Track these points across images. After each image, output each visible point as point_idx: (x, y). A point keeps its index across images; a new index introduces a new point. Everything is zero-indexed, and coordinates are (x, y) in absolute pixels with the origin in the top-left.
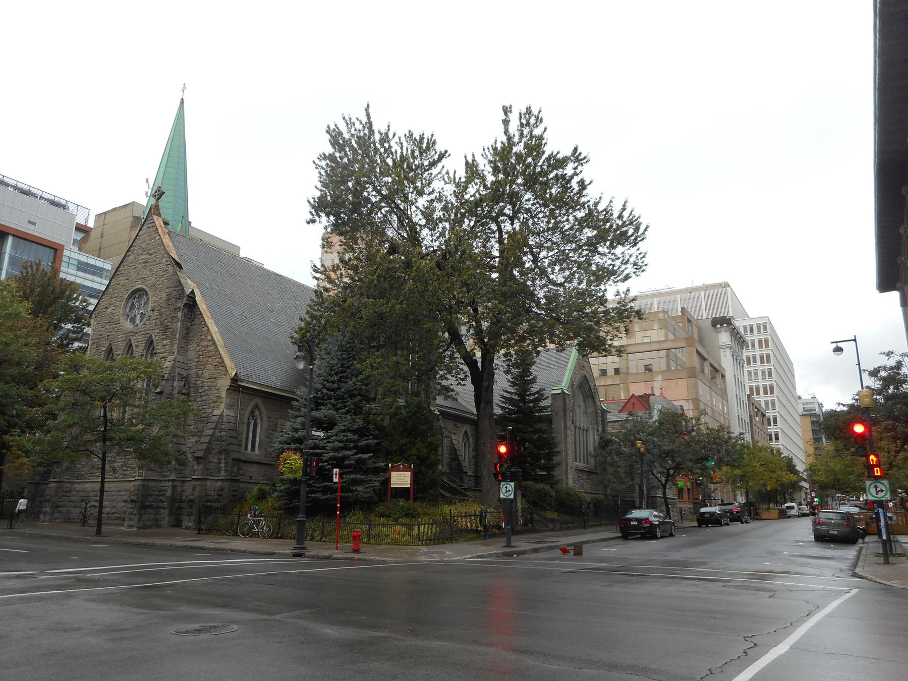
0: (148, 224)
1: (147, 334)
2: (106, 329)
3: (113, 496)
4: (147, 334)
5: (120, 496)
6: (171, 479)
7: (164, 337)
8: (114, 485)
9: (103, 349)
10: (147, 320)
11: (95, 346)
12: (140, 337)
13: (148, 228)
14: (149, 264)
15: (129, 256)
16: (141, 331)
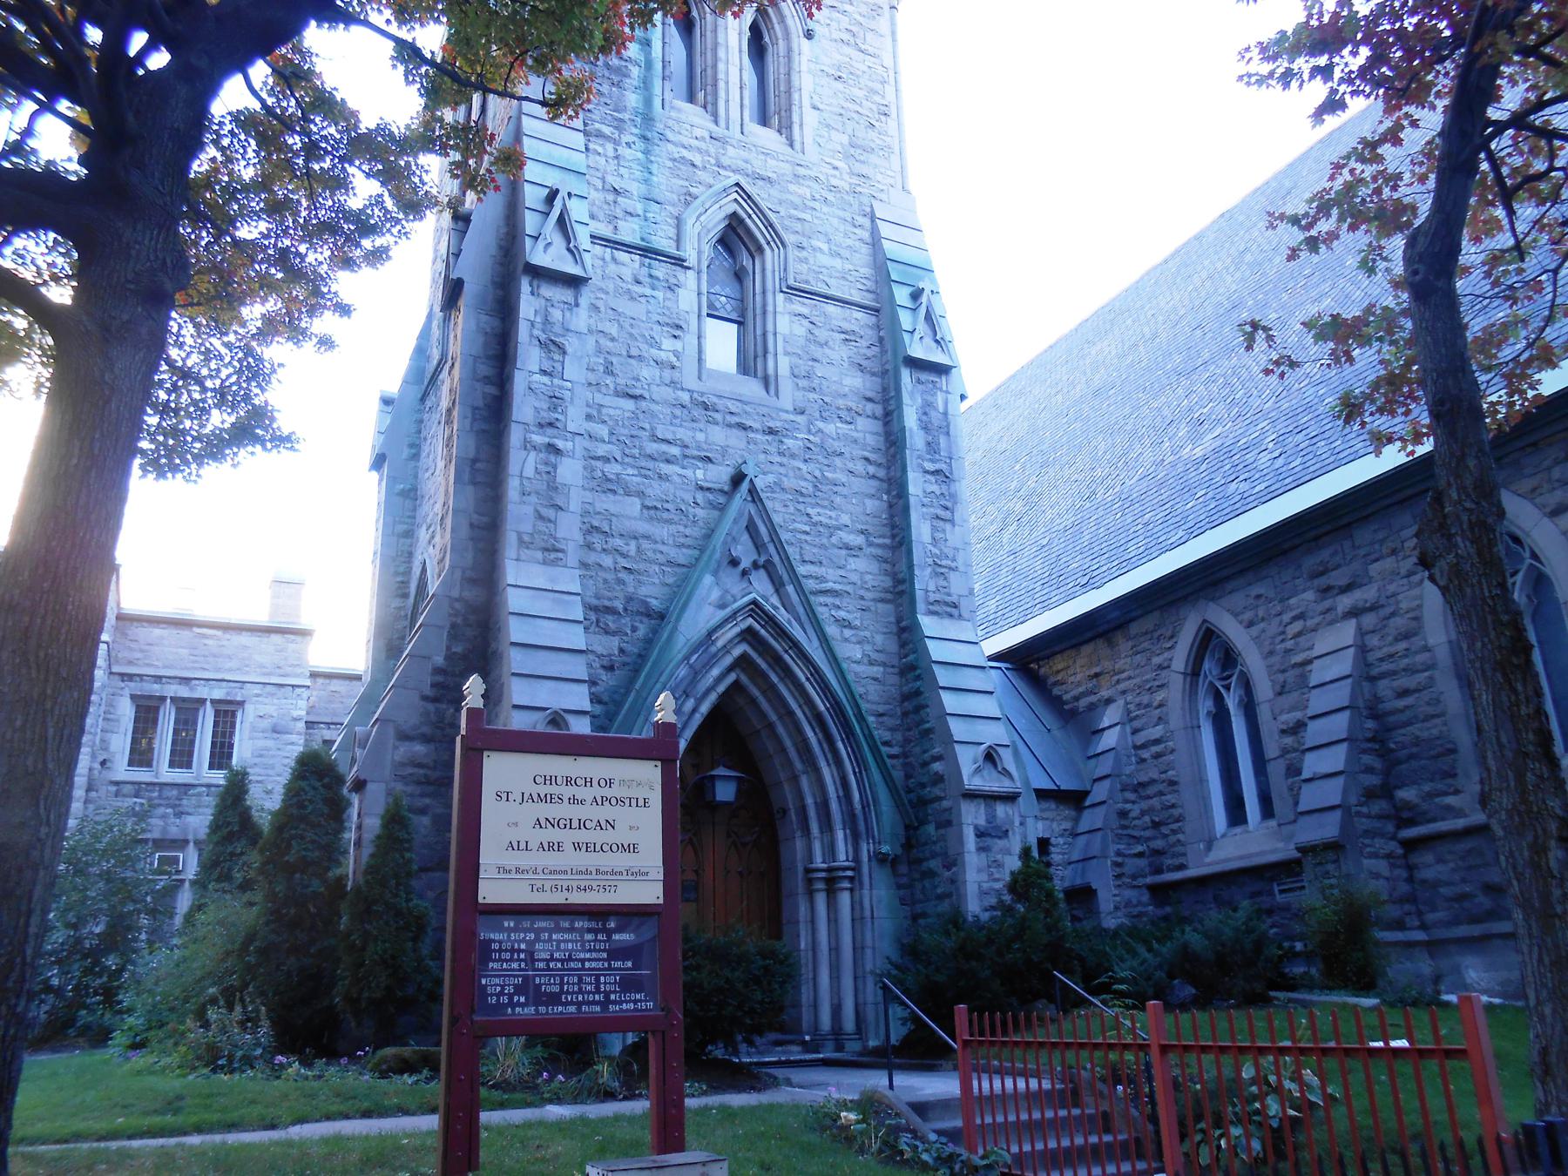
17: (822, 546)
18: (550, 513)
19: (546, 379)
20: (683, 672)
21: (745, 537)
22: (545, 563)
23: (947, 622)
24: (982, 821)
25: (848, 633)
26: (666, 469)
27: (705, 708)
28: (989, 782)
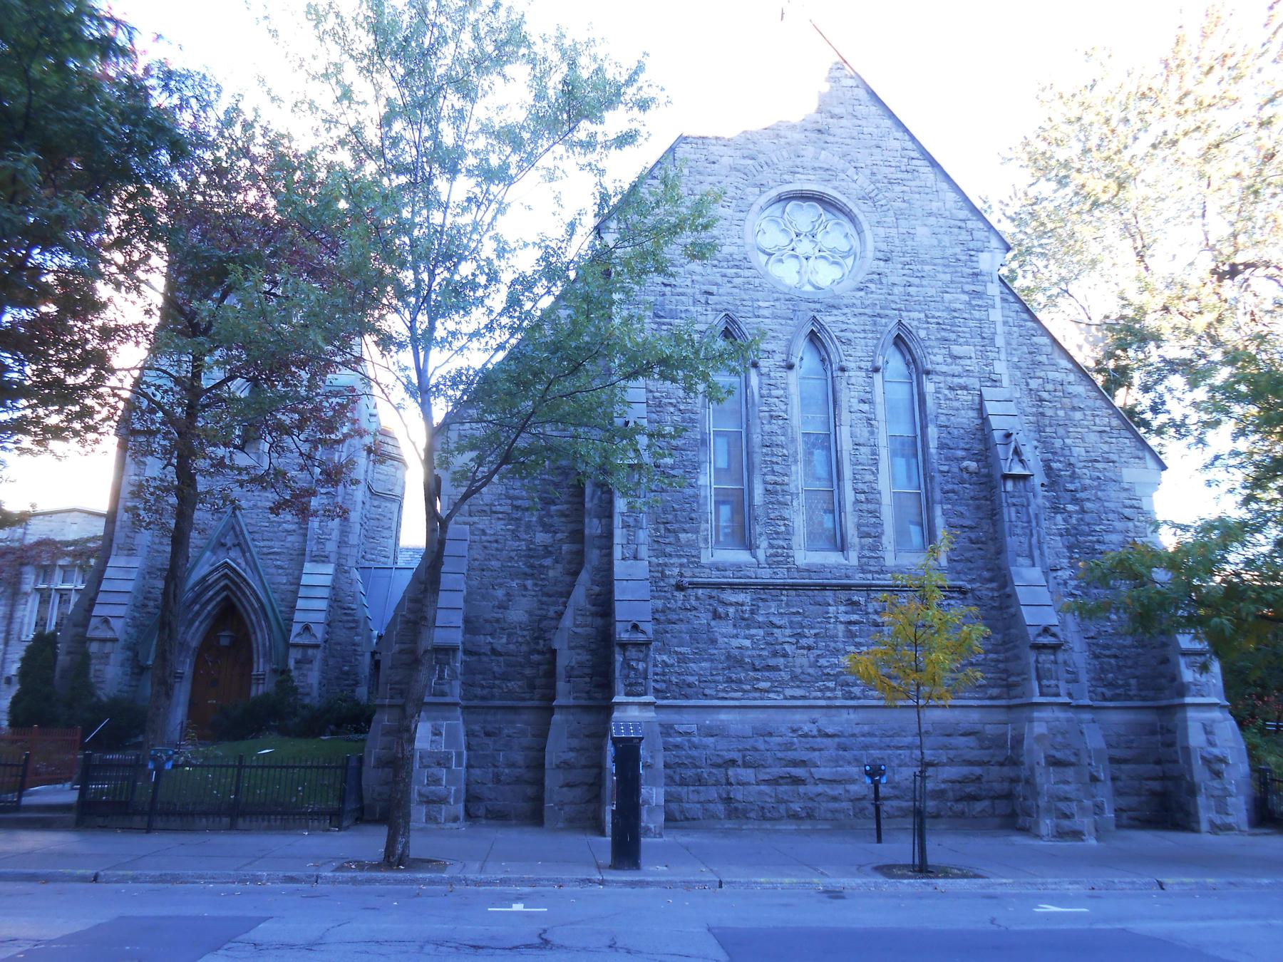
1: (879, 315)
2: (692, 273)
3: (866, 747)
4: (879, 315)
6: (1081, 702)
7: (953, 336)
8: (845, 716)
10: (871, 281)
12: (854, 320)
14: (830, 139)
17: (275, 532)
18: (132, 535)
19: (137, 478)
20: (190, 595)
21: (232, 532)
22: (128, 555)
23: (320, 565)
25: (280, 571)
27: (209, 608)
28: (305, 640)
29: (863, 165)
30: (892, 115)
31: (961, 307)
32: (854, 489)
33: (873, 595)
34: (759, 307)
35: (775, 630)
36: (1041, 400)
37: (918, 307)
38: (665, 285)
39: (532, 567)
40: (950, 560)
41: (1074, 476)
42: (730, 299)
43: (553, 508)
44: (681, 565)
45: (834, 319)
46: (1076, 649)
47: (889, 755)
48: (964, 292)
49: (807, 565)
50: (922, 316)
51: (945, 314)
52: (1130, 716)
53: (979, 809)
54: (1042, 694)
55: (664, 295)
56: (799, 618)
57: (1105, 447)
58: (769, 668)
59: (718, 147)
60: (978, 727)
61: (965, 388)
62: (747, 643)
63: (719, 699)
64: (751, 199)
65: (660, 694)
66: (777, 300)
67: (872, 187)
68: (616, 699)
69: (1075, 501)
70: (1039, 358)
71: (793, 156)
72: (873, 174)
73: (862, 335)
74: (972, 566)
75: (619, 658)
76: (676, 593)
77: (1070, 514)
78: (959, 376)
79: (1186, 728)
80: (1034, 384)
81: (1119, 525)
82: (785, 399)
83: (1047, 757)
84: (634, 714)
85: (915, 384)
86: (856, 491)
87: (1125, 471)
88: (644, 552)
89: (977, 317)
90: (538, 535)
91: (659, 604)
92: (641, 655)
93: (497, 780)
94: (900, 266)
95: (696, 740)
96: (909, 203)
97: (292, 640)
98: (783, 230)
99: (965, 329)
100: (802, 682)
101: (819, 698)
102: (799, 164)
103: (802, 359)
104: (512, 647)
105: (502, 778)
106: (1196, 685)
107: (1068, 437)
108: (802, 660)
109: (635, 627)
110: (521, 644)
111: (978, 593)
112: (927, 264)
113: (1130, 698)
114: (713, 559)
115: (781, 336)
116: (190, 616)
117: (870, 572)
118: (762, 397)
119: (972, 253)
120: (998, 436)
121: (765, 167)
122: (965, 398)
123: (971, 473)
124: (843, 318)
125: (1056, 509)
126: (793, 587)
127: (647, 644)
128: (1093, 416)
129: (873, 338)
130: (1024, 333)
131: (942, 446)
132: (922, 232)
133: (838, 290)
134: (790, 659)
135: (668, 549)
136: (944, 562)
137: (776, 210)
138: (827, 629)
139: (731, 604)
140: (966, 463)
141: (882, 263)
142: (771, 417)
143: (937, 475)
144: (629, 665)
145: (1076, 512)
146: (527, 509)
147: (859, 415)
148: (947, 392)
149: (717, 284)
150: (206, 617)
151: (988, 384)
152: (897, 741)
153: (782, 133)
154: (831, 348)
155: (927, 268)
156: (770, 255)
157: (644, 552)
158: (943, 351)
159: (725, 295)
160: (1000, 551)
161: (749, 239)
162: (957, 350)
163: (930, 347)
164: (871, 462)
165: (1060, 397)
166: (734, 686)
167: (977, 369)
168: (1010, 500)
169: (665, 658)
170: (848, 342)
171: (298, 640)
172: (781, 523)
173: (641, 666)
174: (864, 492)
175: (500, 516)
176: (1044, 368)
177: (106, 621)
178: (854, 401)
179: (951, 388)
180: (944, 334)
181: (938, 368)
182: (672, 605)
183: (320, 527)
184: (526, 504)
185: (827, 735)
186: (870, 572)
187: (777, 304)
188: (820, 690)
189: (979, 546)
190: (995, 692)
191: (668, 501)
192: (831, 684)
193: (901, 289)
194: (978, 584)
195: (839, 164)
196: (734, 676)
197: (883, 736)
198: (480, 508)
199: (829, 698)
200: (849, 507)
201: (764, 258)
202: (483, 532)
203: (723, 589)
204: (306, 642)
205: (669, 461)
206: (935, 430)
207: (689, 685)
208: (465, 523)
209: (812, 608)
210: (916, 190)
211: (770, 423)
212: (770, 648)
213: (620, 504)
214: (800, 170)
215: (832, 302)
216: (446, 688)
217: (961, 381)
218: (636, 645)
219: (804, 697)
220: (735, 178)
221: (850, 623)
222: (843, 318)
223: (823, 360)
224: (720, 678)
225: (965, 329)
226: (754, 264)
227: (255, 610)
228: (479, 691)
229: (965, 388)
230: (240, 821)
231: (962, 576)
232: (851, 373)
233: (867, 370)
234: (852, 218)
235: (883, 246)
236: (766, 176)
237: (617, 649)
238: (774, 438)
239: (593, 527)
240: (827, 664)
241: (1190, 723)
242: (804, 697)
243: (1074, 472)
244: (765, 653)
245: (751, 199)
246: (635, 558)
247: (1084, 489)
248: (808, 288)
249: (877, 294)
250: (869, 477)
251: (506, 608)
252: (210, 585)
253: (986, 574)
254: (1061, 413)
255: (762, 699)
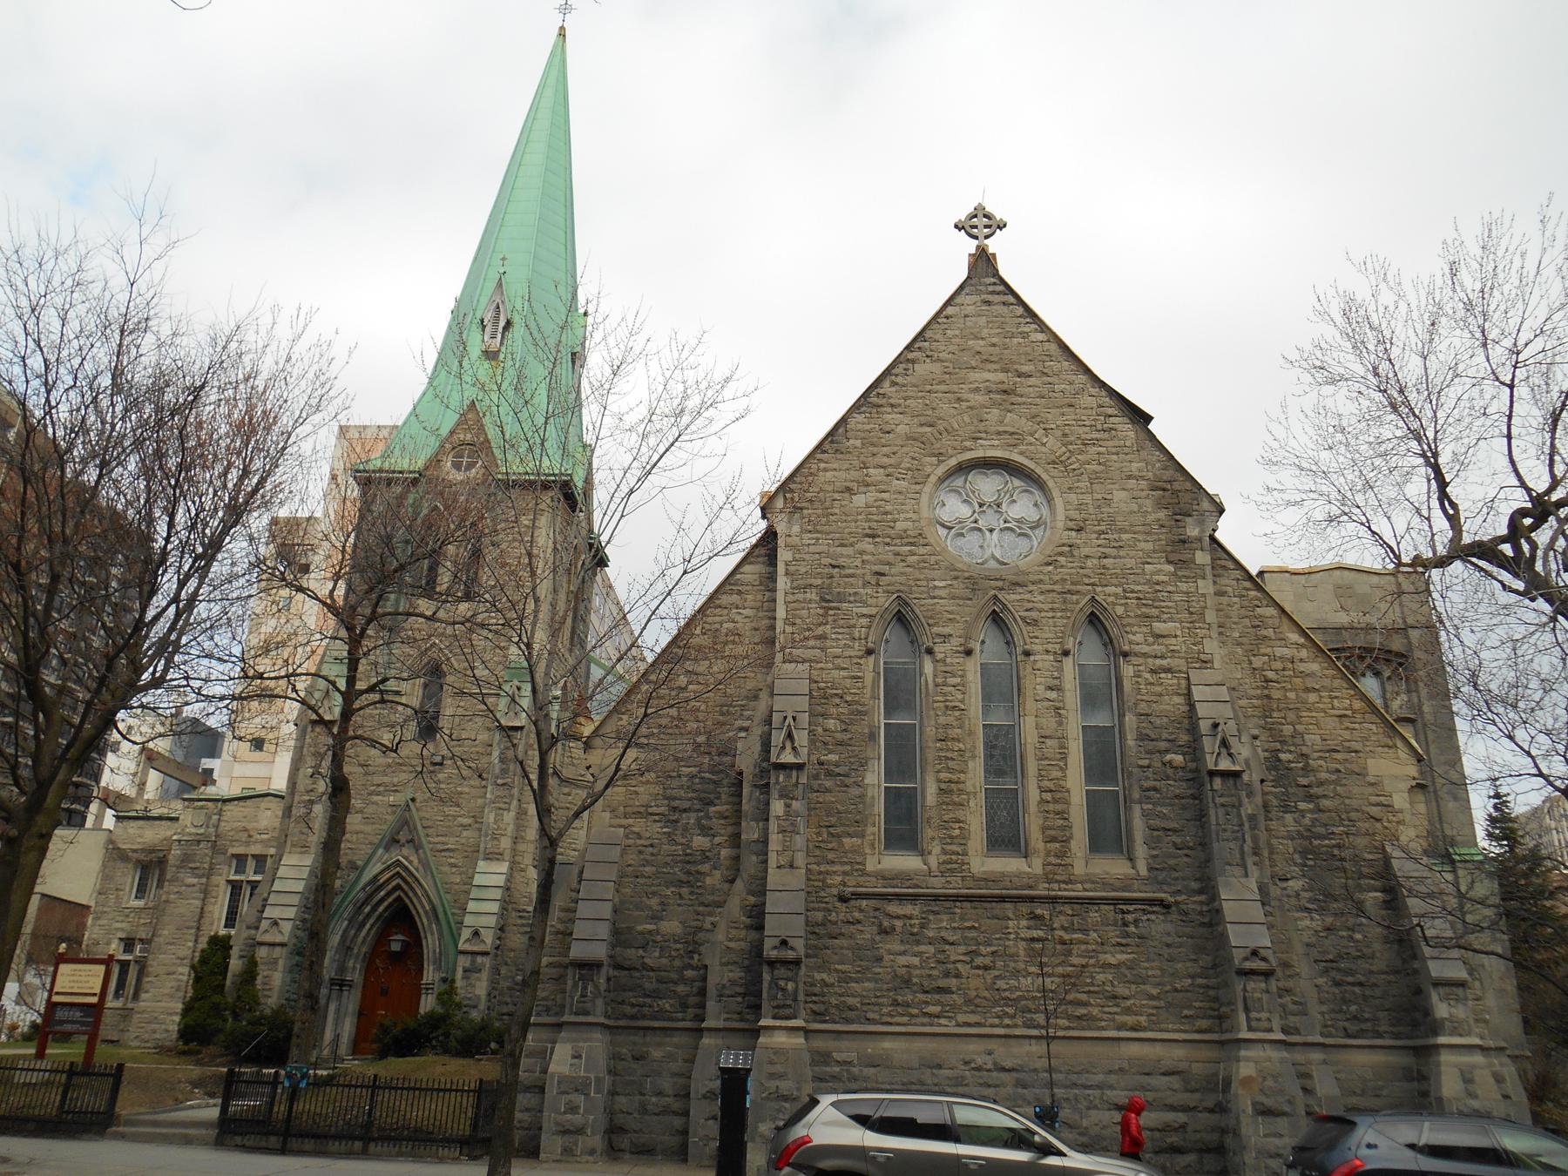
0: (979, 292)
1: (1069, 592)
2: (862, 553)
4: (1069, 592)
5: (1086, 1087)
6: (1310, 1039)
7: (1155, 612)
9: (865, 611)
10: (1061, 554)
11: (812, 595)
12: (1041, 598)
13: (988, 303)
14: (1020, 400)
15: (913, 362)
16: (1041, 581)
17: (449, 827)
20: (362, 895)
24: (467, 965)
25: (454, 870)
26: (375, 798)
27: (381, 909)
29: (1053, 426)
30: (1087, 371)
31: (1165, 578)
32: (1040, 787)
33: (1059, 908)
34: (936, 587)
35: (947, 947)
36: (1267, 681)
37: (1114, 581)
38: (834, 567)
39: (689, 873)
40: (1150, 869)
41: (1307, 770)
42: (902, 579)
43: (712, 809)
44: (845, 873)
45: (1018, 597)
46: (1304, 975)
47: (1076, 1095)
48: (1170, 562)
49: (985, 872)
50: (1119, 590)
51: (1146, 588)
52: (1378, 1058)
53: (1183, 1164)
54: (1250, 1029)
55: (832, 577)
56: (973, 934)
57: (1347, 734)
58: (940, 990)
59: (893, 416)
60: (1182, 1066)
61: (1168, 670)
62: (916, 961)
63: (883, 1024)
64: (928, 469)
65: (818, 1018)
66: (956, 578)
67: (1064, 449)
68: (763, 1022)
69: (1310, 798)
70: (1264, 632)
71: (975, 421)
72: (1065, 435)
73: (1050, 614)
74: (1176, 875)
75: (766, 977)
76: (838, 904)
77: (1303, 813)
78: (1162, 657)
79: (1439, 1074)
80: (1258, 662)
81: (1364, 825)
82: (962, 687)
83: (1254, 1104)
84: (781, 1039)
85: (1112, 667)
86: (1042, 790)
87: (1370, 762)
88: (800, 859)
89: (1185, 589)
90: (695, 838)
91: (819, 916)
92: (790, 974)
93: (644, 1110)
94: (1096, 536)
95: (855, 1070)
96: (1105, 465)
97: (461, 946)
98: (965, 501)
99: (1170, 604)
100: (977, 1006)
101: (997, 1026)
102: (982, 429)
103: (983, 642)
104: (664, 961)
105: (650, 1107)
106: (1452, 1022)
107: (1300, 723)
108: (975, 983)
109: (784, 943)
110: (674, 958)
111: (1184, 907)
112: (1126, 532)
113: (1379, 1035)
114: (879, 867)
115: (958, 617)
116: (361, 918)
117: (1057, 881)
118: (937, 685)
119: (1178, 517)
120: (1204, 726)
121: (945, 434)
122: (1170, 682)
123: (1176, 768)
124: (1027, 596)
125: (1286, 809)
126: (969, 898)
127: (797, 963)
128: (1331, 697)
129: (1061, 617)
130: (1245, 603)
131: (1142, 737)
132: (1119, 495)
133: (1022, 564)
134: (964, 980)
135: (831, 856)
136: (1143, 871)
137: (959, 482)
138: (1006, 947)
139: (898, 917)
140: (1169, 757)
141: (1073, 534)
142: (947, 707)
143: (1135, 770)
144: (776, 984)
145: (1310, 811)
146: (685, 811)
147: (1046, 704)
148: (1148, 675)
149: (889, 564)
150: (377, 920)
151: (1197, 665)
152: (1082, 1080)
153: (965, 396)
154: (1015, 629)
155: (1125, 536)
156: (950, 528)
157: (800, 859)
158: (1144, 629)
159: (897, 575)
160: (1208, 860)
161: (925, 513)
162: (1159, 627)
163: (1129, 625)
164: (1058, 756)
165: (1290, 676)
166: (900, 1009)
167: (1184, 649)
168: (1218, 800)
169: (824, 976)
170: (1035, 623)
171: (467, 947)
172: (957, 825)
173: (790, 986)
174: (1051, 791)
175: (657, 818)
176: (1268, 643)
177: (275, 923)
178: (1040, 688)
179: (1152, 671)
180: (1144, 610)
181: (1137, 648)
182: (833, 917)
183: (496, 822)
184: (686, 805)
185: (1004, 1069)
186: (1057, 881)
187: (955, 582)
188: (999, 1017)
189: (1186, 851)
190: (1204, 1024)
191: (833, 802)
192: (1010, 1010)
193: (1095, 561)
194: (1184, 897)
195: (1026, 426)
196: (900, 999)
197: (1069, 1072)
198: (635, 810)
199: (1008, 1026)
200: (1033, 807)
201: (942, 532)
202: (639, 836)
203: (890, 900)
204: (475, 948)
205: (833, 757)
206: (1134, 718)
207: (851, 1009)
208: (621, 826)
209: (988, 921)
210: (1114, 450)
211: (945, 714)
212: (942, 967)
213: (777, 807)
214: (983, 435)
215: (1020, 579)
216: (588, 1006)
217: (1164, 662)
218: (785, 963)
219: (978, 1024)
220: (913, 449)
221: (1033, 940)
222: (1027, 596)
223: (1007, 643)
224: (884, 1000)
225: (1170, 604)
226: (932, 541)
227: (426, 913)
228: (628, 1010)
229: (1168, 670)
230: (372, 1146)
231: (1165, 887)
232: (1037, 657)
233: (1055, 653)
234: (1040, 485)
235: (1074, 514)
236: (946, 442)
237: (765, 968)
238: (949, 732)
239: (750, 832)
240: (1005, 987)
241: (1443, 1068)
242: (978, 1024)
243: (1307, 764)
244: (935, 972)
245: (928, 469)
246: (791, 866)
247: (1321, 784)
248: (992, 564)
249: (1068, 568)
250: (1056, 774)
251: (661, 919)
252: (381, 885)
253: (1195, 885)
254: (1292, 695)
255: (931, 1025)
